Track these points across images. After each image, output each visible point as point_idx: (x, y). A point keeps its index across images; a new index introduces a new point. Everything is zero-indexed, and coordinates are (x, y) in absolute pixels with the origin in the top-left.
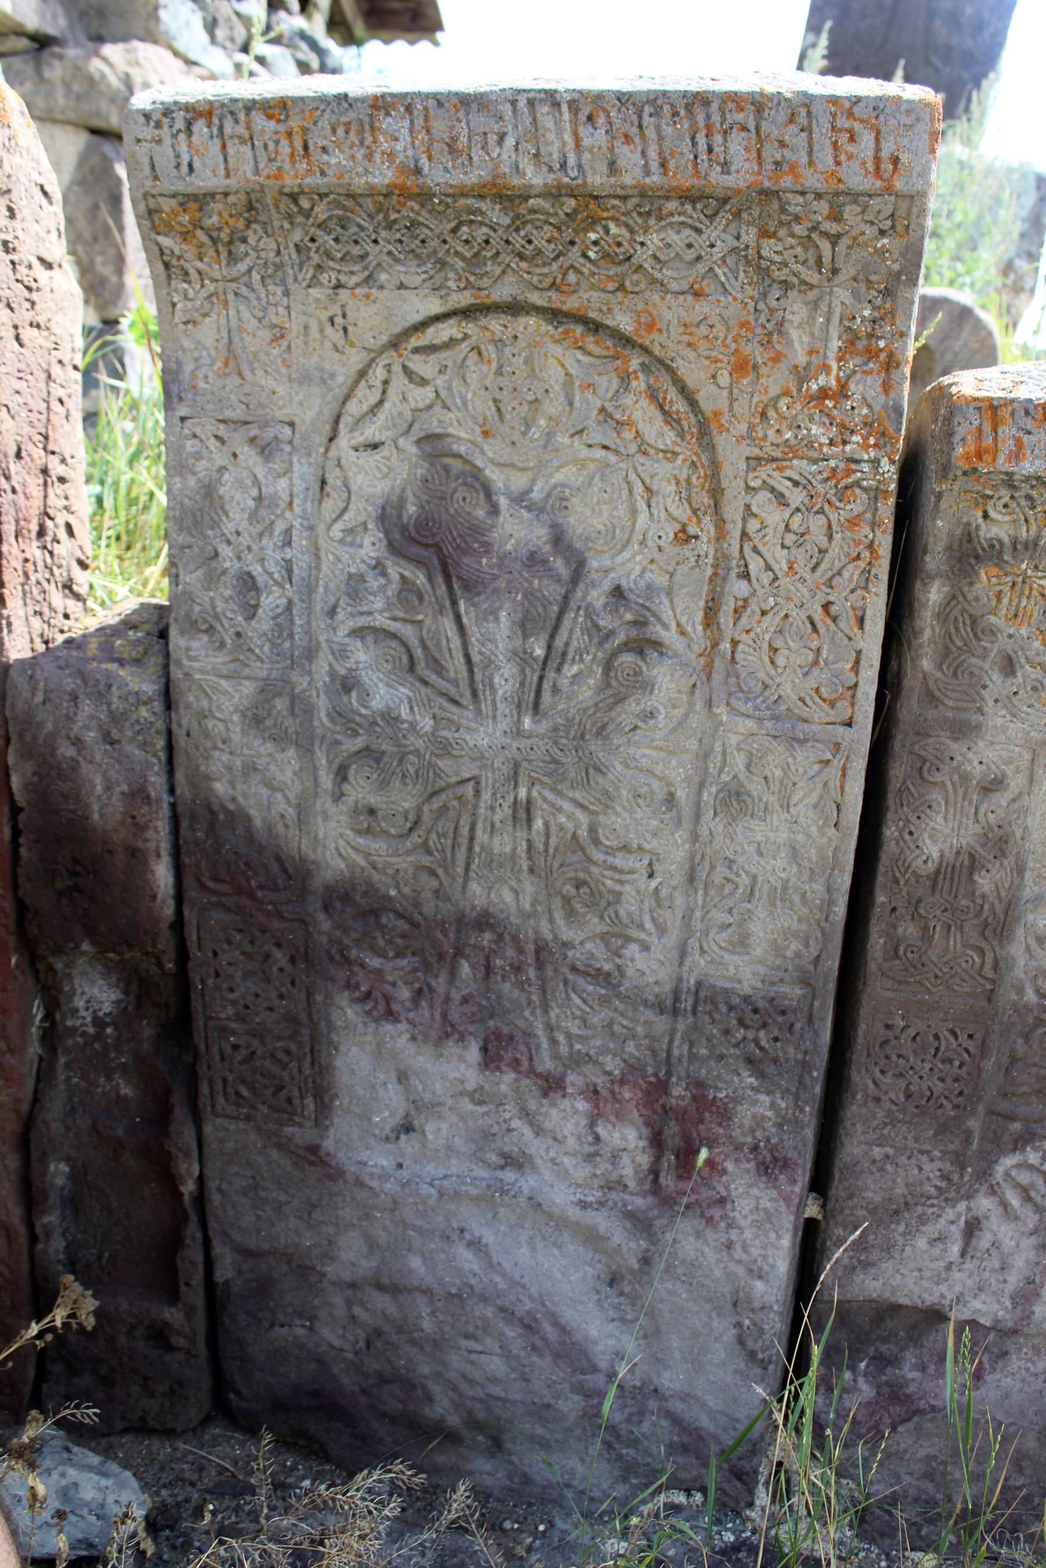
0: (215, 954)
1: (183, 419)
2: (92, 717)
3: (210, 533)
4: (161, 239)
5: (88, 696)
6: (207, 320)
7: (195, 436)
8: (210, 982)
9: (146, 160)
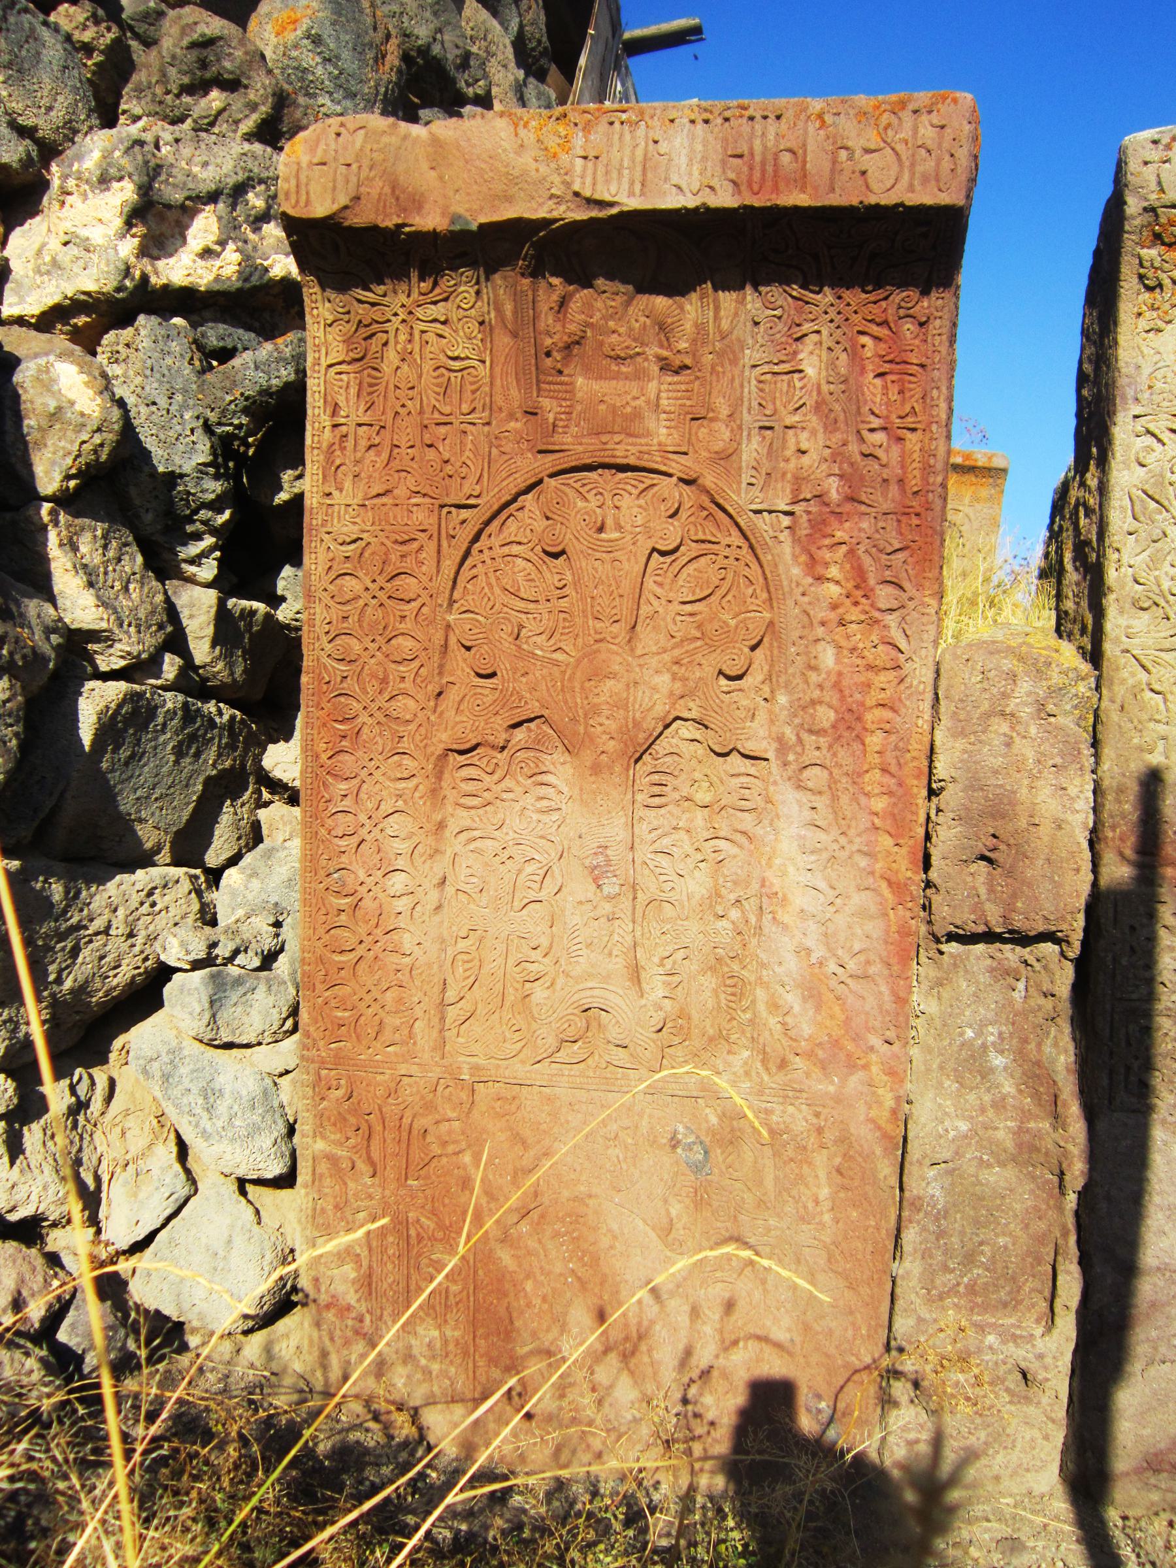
0: (1133, 928)
1: (1136, 417)
2: (1029, 694)
3: (1158, 517)
4: (1146, 253)
5: (1027, 674)
6: (1170, 326)
7: (1148, 432)
8: (1124, 961)
9: (1153, 179)
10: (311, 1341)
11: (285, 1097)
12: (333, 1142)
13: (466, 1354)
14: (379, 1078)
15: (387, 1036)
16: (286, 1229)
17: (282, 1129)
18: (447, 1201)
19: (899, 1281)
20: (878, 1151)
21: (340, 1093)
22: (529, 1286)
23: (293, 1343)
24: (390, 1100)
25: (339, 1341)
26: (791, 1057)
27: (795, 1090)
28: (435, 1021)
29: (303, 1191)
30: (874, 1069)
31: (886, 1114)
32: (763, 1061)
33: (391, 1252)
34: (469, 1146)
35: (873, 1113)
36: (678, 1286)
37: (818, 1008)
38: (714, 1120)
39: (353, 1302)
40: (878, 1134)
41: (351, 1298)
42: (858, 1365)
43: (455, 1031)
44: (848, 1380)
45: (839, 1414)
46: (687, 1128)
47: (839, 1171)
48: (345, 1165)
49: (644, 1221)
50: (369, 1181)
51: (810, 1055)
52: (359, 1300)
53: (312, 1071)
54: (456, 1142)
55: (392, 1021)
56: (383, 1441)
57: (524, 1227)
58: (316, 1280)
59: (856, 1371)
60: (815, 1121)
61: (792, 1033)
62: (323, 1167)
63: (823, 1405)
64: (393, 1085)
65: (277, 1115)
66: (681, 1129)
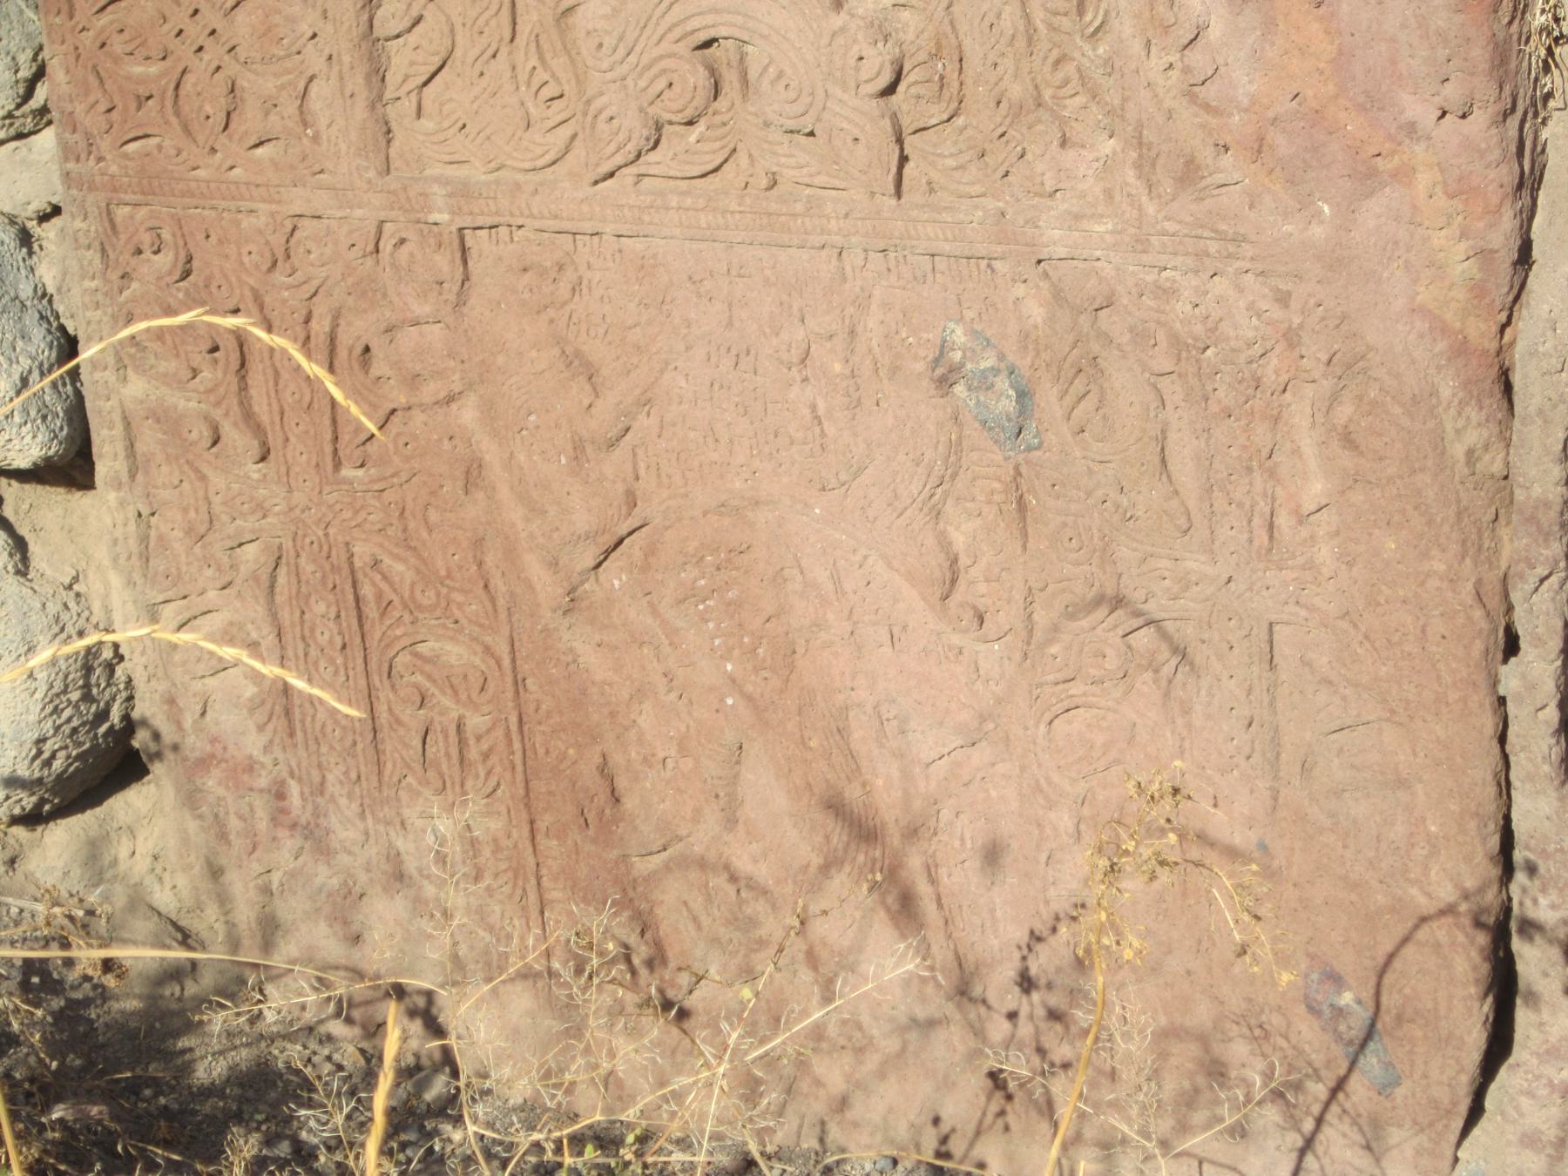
10: (185, 840)
11: (48, 274)
12: (165, 378)
13: (517, 871)
14: (247, 222)
15: (250, 121)
16: (91, 586)
17: (39, 343)
18: (433, 516)
19: (1511, 708)
20: (1447, 388)
21: (164, 260)
22: (646, 718)
23: (145, 846)
24: (279, 277)
25: (238, 844)
26: (1206, 155)
27: (1221, 237)
28: (357, 82)
29: (112, 496)
30: (1424, 180)
31: (1460, 294)
32: (1138, 166)
33: (323, 640)
34: (470, 386)
35: (1424, 296)
36: (983, 719)
37: (1269, 24)
38: (1035, 312)
39: (256, 753)
40: (1441, 346)
41: (254, 745)
42: (1425, 905)
43: (409, 105)
44: (1405, 940)
45: (1386, 1019)
46: (973, 333)
47: (1348, 441)
48: (200, 433)
49: (889, 565)
50: (254, 471)
51: (1259, 148)
52: (267, 749)
53: (93, 211)
54: (439, 374)
55: (258, 84)
56: (791, 1143)
57: (615, 576)
58: (171, 701)
59: (1424, 919)
60: (1277, 313)
61: (1210, 93)
62: (149, 439)
63: (1347, 998)
64: (278, 240)
65: (31, 319)
66: (959, 335)
